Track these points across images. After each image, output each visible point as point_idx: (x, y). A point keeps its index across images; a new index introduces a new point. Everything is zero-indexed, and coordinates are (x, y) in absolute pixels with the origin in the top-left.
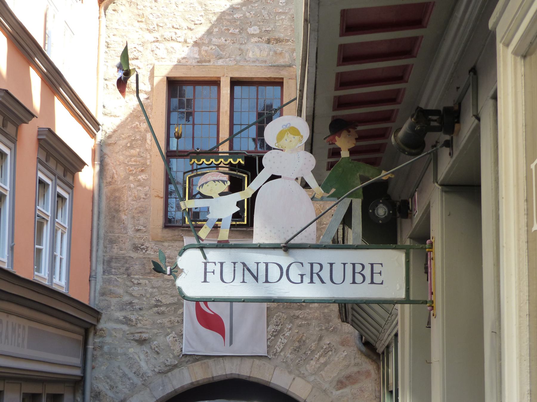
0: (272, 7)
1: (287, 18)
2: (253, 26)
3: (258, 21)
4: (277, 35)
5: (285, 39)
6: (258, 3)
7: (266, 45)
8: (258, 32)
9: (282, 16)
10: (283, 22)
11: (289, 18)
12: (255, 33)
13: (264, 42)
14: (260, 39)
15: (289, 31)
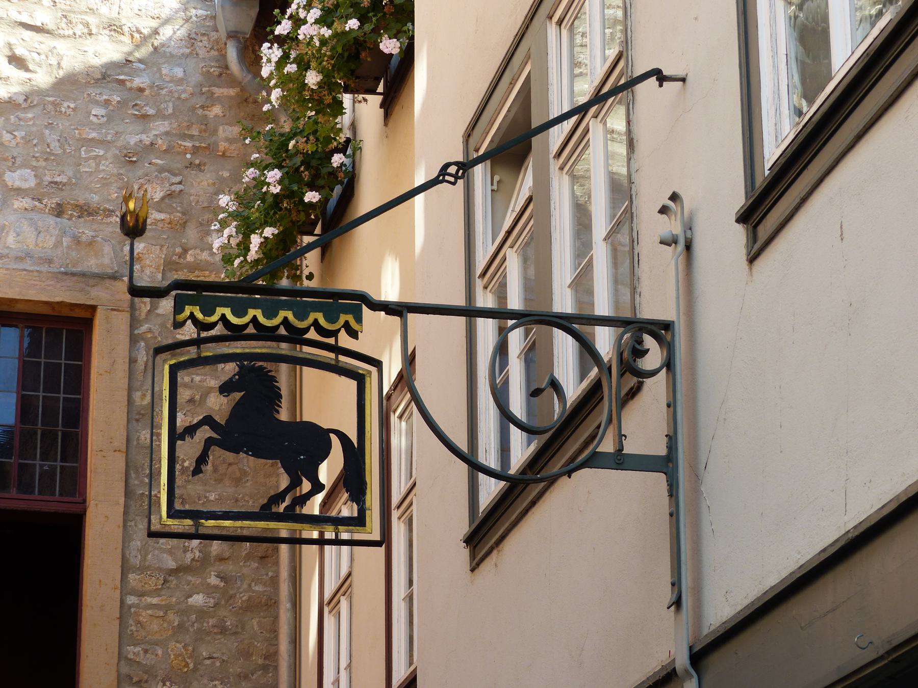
0: (71, 125)
1: (109, 155)
2: (20, 167)
3: (34, 157)
4: (82, 197)
5: (102, 208)
6: (35, 110)
7: (52, 220)
8: (32, 183)
9: (97, 150)
10: (98, 165)
11: (115, 156)
12: (25, 185)
13: (47, 210)
14: (36, 203)
15: (113, 188)
